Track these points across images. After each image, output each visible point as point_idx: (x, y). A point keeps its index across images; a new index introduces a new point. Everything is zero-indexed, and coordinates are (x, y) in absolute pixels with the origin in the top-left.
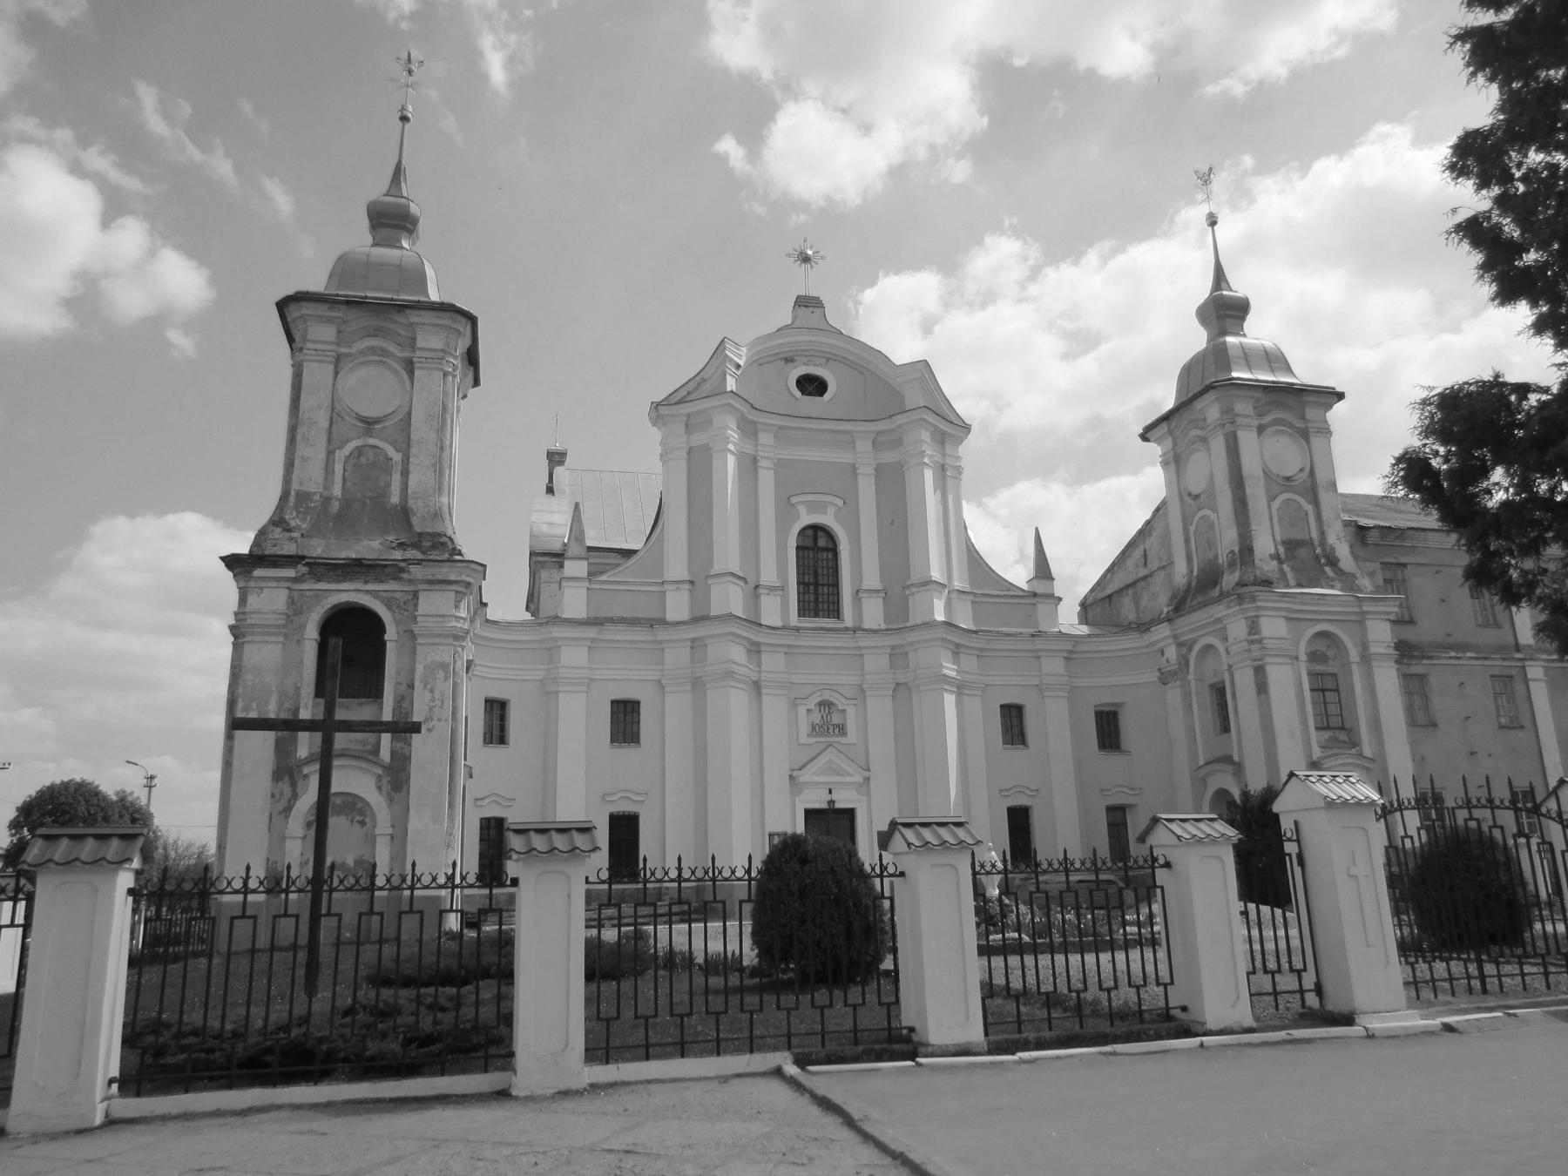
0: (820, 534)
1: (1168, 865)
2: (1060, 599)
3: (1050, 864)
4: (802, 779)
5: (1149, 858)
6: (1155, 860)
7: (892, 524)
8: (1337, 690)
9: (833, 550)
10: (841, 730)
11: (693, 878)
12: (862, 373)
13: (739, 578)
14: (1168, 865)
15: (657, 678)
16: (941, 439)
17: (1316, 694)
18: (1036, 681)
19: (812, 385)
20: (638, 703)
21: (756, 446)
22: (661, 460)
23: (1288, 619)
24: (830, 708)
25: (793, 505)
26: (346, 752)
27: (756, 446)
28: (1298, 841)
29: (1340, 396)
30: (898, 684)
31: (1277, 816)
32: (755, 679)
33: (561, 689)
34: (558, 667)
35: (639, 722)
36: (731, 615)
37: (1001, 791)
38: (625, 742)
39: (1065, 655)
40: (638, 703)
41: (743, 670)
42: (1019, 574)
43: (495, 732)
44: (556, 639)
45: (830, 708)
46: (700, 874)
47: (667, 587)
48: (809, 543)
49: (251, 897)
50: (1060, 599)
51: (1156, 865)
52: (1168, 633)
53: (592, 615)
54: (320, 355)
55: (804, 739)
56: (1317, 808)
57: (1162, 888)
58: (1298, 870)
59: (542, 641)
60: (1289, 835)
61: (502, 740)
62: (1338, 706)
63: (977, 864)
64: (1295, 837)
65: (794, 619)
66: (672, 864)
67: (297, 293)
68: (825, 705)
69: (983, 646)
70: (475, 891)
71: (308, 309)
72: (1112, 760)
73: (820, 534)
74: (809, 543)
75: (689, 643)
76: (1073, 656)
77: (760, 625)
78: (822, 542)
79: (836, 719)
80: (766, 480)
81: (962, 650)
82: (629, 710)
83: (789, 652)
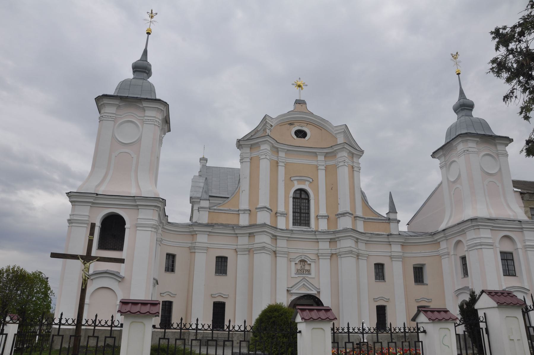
0: (303, 192)
1: (424, 332)
2: (399, 221)
3: (369, 330)
4: (292, 292)
5: (416, 328)
6: (418, 329)
7: (332, 189)
8: (513, 260)
9: (308, 200)
10: (309, 272)
11: (239, 330)
12: (321, 130)
13: (268, 209)
14: (424, 332)
15: (235, 248)
16: (352, 155)
17: (504, 261)
18: (389, 254)
19: (301, 134)
20: (227, 258)
21: (278, 157)
22: (240, 162)
23: (491, 230)
24: (304, 263)
25: (292, 181)
26: (107, 271)
27: (278, 157)
28: (486, 322)
29: (511, 140)
30: (332, 254)
31: (476, 310)
32: (274, 250)
33: (196, 251)
34: (196, 242)
35: (227, 266)
36: (265, 224)
37: (374, 299)
38: (221, 273)
39: (401, 244)
40: (227, 258)
41: (270, 247)
42: (384, 211)
43: (170, 267)
44: (195, 231)
45: (304, 263)
46: (206, 327)
47: (240, 212)
48: (298, 196)
49: (62, 327)
50: (399, 221)
51: (419, 331)
52: (443, 235)
53: (210, 222)
54: (109, 118)
55: (293, 275)
56: (494, 307)
57: (422, 342)
58: (486, 336)
59: (190, 232)
60: (481, 319)
61: (173, 270)
62: (513, 266)
63: (335, 329)
64: (484, 321)
65: (291, 226)
66: (194, 322)
67: (102, 95)
68: (303, 261)
69: (368, 239)
70: (159, 330)
71: (105, 101)
72: (420, 287)
73: (303, 192)
74: (298, 196)
75: (248, 235)
76: (405, 244)
77: (277, 228)
78: (303, 196)
79: (307, 267)
80: (281, 170)
81: (359, 241)
82: (223, 260)
83: (289, 239)
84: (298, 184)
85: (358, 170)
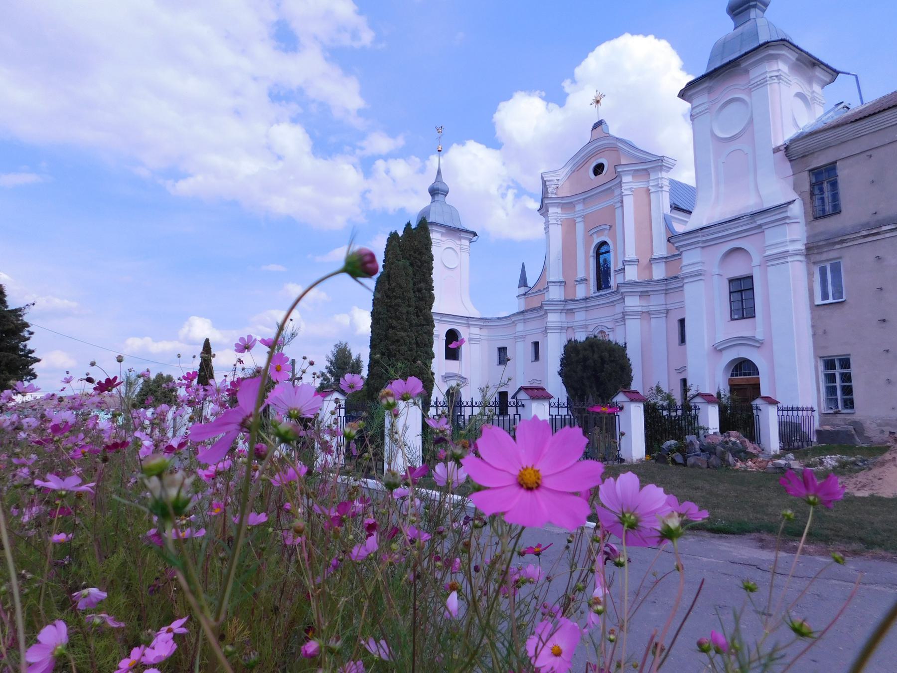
69: (664, 288)
84: (597, 237)
85: (660, 189)
